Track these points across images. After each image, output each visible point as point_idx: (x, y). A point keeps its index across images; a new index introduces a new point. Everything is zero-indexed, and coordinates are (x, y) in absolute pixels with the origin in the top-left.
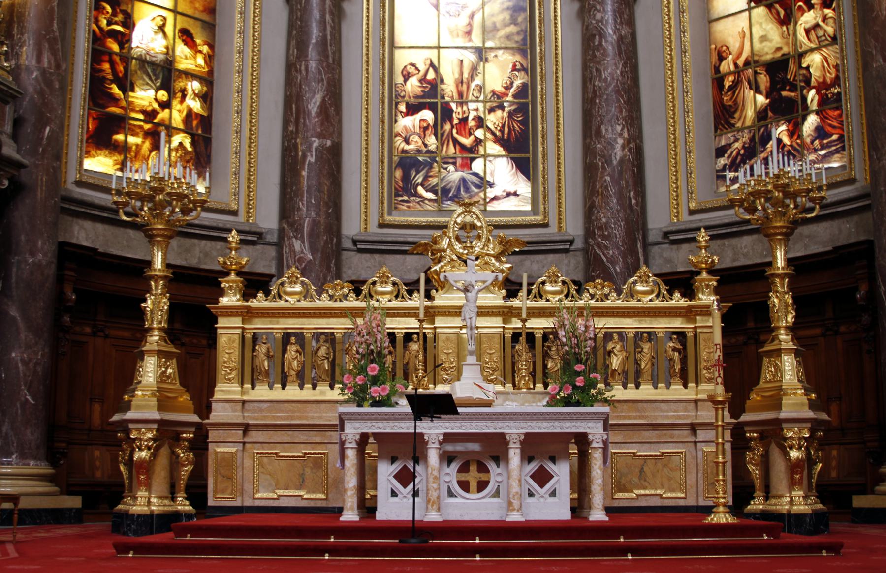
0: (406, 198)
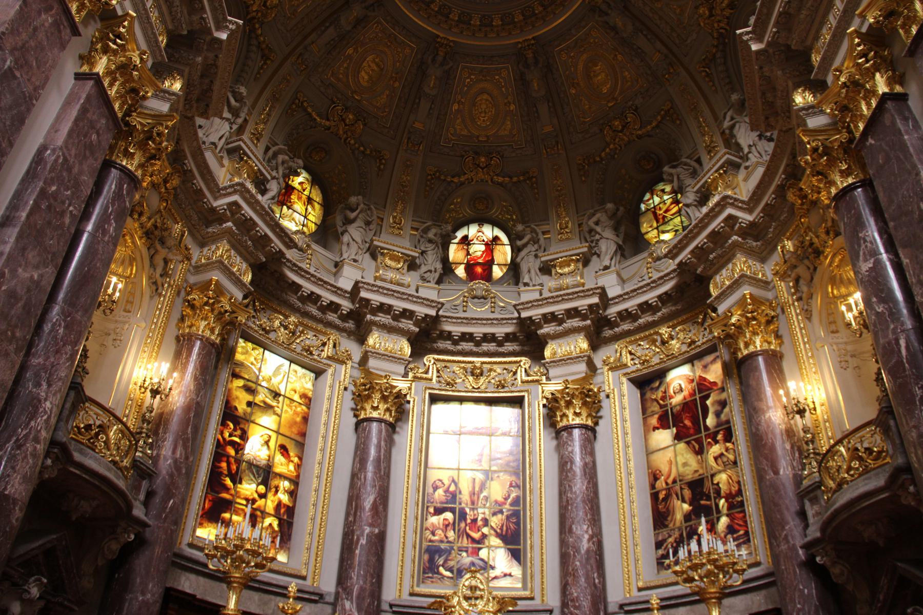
0: (430, 575)
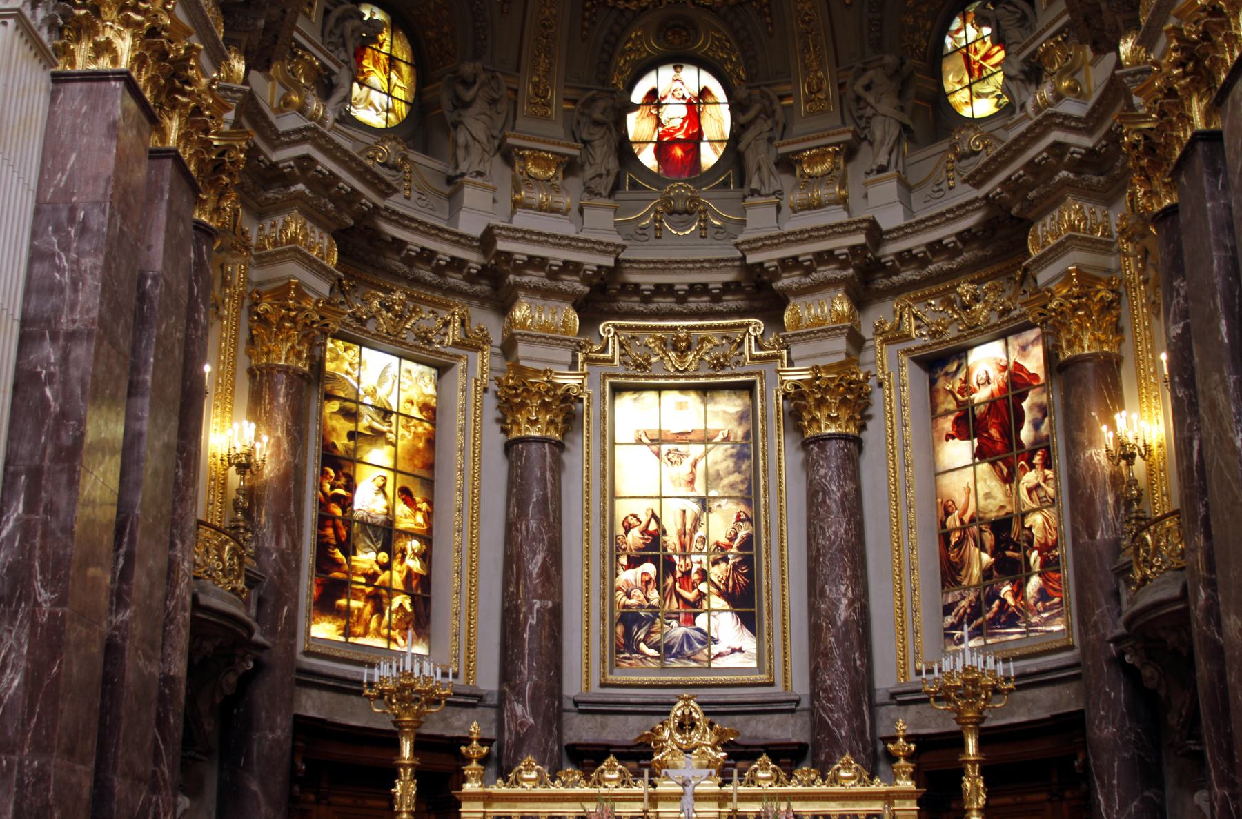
0: (627, 655)
